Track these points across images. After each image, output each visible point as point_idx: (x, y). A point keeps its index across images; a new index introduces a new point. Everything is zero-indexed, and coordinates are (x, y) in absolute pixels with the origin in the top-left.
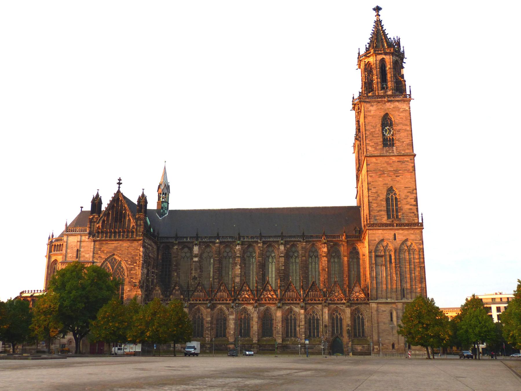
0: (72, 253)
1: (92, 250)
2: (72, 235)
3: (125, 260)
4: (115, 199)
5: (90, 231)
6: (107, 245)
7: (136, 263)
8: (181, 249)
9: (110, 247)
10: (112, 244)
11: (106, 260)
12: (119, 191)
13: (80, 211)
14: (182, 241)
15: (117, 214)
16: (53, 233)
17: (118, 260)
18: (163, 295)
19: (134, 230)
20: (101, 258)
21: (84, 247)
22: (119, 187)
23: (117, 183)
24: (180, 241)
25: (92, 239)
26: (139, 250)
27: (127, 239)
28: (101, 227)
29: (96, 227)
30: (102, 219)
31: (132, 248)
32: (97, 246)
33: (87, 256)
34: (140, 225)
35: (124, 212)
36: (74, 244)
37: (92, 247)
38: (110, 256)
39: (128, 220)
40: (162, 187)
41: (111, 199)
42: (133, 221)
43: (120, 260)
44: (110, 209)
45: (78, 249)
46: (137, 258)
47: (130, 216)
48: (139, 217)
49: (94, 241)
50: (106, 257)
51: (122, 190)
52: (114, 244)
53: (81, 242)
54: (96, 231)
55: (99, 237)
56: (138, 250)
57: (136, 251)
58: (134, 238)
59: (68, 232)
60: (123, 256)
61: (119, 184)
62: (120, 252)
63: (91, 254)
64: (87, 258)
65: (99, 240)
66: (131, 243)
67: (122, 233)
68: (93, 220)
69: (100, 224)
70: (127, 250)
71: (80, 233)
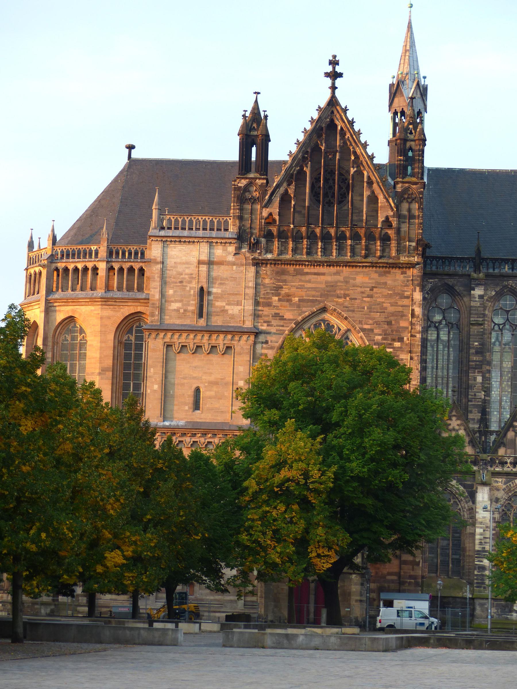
0: (181, 301)
1: (251, 292)
2: (179, 240)
3: (363, 330)
4: (321, 129)
5: (240, 228)
6: (299, 277)
7: (401, 340)
8: (491, 298)
9: (309, 285)
10: (315, 274)
11: (299, 325)
12: (333, 102)
13: (125, 160)
14: (497, 271)
15: (329, 173)
16: (53, 230)
17: (340, 330)
18: (473, 446)
19: (390, 232)
20: (282, 318)
21: (223, 282)
22: (334, 88)
23: (327, 75)
24: (491, 271)
25: (248, 255)
26: (411, 298)
27: (369, 259)
28: (277, 218)
29: (261, 218)
30: (282, 190)
31: (386, 292)
32: (267, 281)
33: (233, 310)
34: (412, 217)
35: (352, 171)
36: (187, 271)
37: (251, 284)
38: (313, 315)
39: (369, 197)
40: (409, 91)
41: (309, 127)
42: (388, 201)
43: (344, 327)
44: (304, 159)
45: (202, 289)
46: (404, 324)
47: (375, 186)
48: (405, 190)
49: (257, 263)
50: (300, 318)
51: (343, 101)
52: (323, 274)
53: (210, 263)
54: (260, 230)
55: (271, 252)
56: (408, 297)
57: (400, 303)
58: (390, 257)
59: (163, 228)
60: (357, 316)
61: (334, 75)
62: (346, 304)
63: (249, 306)
64: (232, 317)
65: (275, 262)
66: (380, 275)
67: (349, 242)
68: (248, 195)
69: (275, 209)
70: (368, 296)
71: (208, 233)
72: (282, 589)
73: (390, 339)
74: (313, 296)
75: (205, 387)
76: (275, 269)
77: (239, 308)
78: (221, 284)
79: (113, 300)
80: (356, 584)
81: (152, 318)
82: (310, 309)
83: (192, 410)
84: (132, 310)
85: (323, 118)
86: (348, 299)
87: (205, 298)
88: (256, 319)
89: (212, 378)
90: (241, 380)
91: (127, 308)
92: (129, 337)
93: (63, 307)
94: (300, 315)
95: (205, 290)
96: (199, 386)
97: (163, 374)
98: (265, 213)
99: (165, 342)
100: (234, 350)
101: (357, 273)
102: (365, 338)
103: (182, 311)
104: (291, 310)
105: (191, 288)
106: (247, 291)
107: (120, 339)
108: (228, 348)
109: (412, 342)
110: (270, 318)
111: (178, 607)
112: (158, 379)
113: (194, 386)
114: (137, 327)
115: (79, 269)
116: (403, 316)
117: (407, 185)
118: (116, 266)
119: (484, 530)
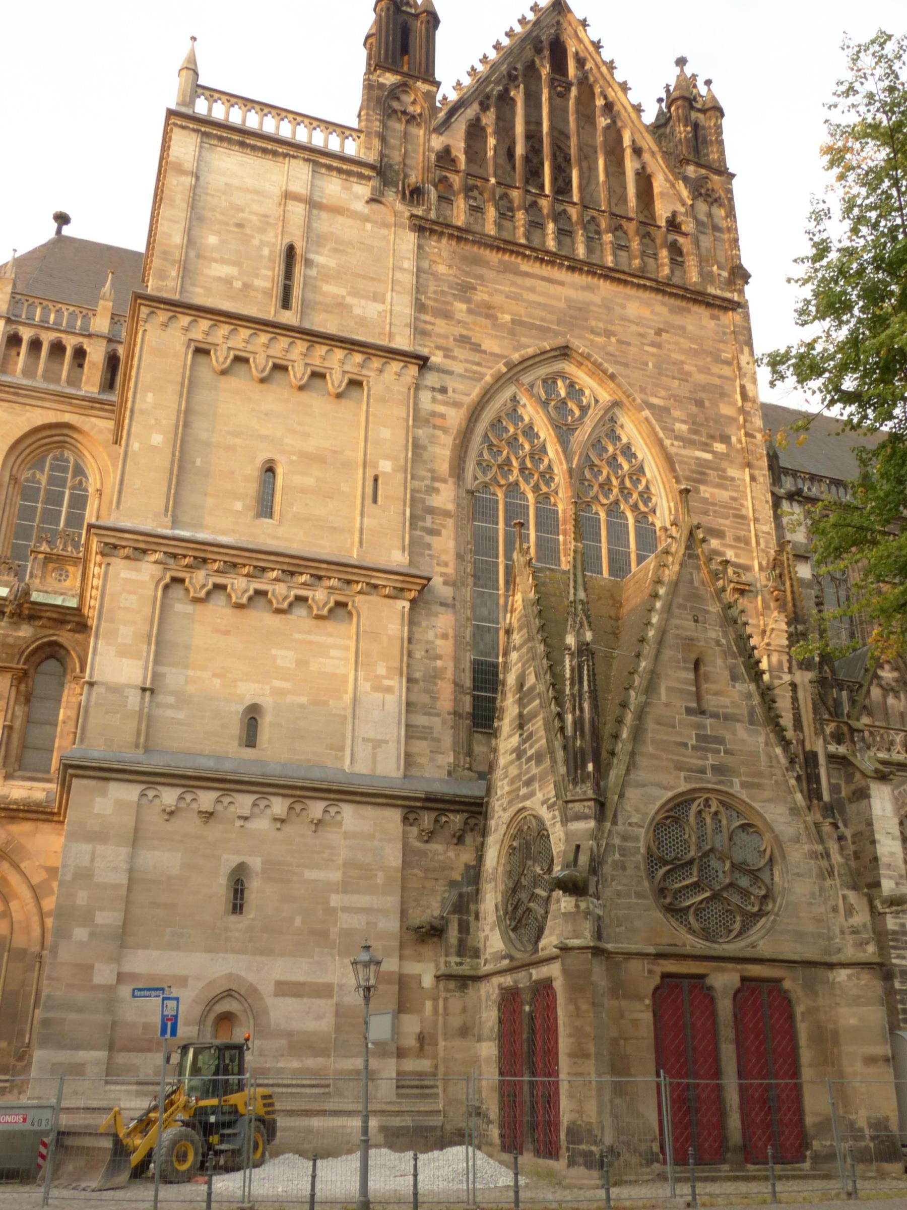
0: (236, 263)
1: (407, 280)
3: (651, 406)
6: (511, 277)
7: (725, 439)
9: (532, 297)
10: (544, 279)
20: (476, 348)
28: (462, 158)
31: (686, 344)
32: (442, 269)
36: (255, 207)
37: (409, 264)
38: (541, 358)
45: (290, 251)
46: (726, 410)
50: (516, 357)
52: (561, 283)
54: (427, 169)
56: (728, 363)
57: (715, 369)
62: (611, 349)
63: (404, 308)
64: (362, 322)
66: (672, 310)
70: (653, 344)
72: (635, 1023)
73: (704, 434)
74: (542, 319)
75: (292, 463)
76: (458, 250)
77: (380, 307)
78: (336, 250)
79: (12, 390)
80: (856, 1001)
81: (161, 283)
82: (537, 342)
83: (251, 514)
84: (52, 417)
85: (543, 24)
86: (613, 340)
87: (299, 270)
88: (418, 337)
89: (310, 445)
90: (386, 457)
91: (39, 411)
92: (34, 474)
94: (516, 349)
95: (298, 251)
96: (276, 457)
97: (179, 411)
98: (437, 142)
99: (190, 340)
100: (369, 390)
101: (628, 297)
102: (654, 422)
103: (238, 284)
104: (497, 337)
105: (263, 244)
106: (399, 275)
107: (14, 472)
108: (355, 384)
109: (751, 447)
110: (451, 343)
111: (214, 1102)
112: (164, 422)
113: (262, 457)
114: (55, 458)
116: (723, 395)
117: (703, 171)
118: (26, 334)
119: (897, 884)
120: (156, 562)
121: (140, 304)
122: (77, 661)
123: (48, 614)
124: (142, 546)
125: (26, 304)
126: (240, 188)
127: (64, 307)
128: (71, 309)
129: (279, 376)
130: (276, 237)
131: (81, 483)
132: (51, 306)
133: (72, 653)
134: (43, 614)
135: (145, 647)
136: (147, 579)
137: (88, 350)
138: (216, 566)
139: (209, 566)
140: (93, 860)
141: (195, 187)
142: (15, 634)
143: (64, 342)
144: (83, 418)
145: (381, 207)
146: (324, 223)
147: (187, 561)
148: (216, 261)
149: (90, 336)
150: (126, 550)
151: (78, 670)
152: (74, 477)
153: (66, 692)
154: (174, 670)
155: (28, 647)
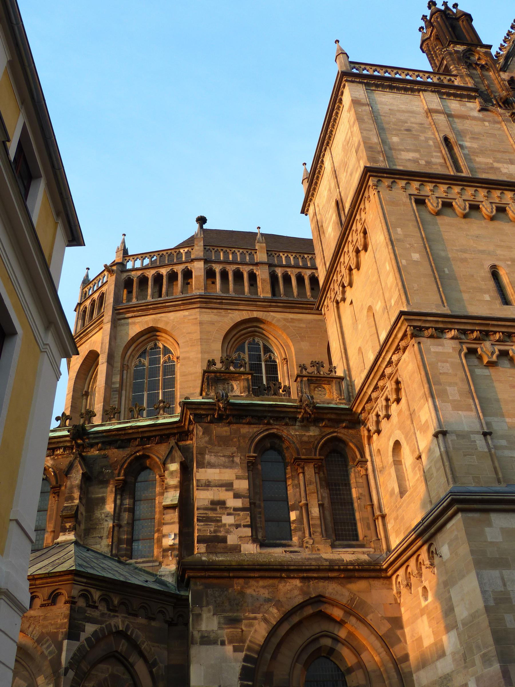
36: (413, 120)
75: (508, 266)
78: (474, 138)
79: (218, 301)
84: (245, 315)
91: (237, 312)
93: (139, 318)
95: (452, 140)
96: (496, 263)
105: (427, 139)
107: (228, 354)
114: (250, 344)
115: (162, 276)
118: (217, 268)
120: (453, 338)
121: (370, 176)
122: (356, 450)
123: (329, 416)
124: (441, 326)
125: (213, 252)
126: (399, 111)
127: (236, 251)
128: (241, 251)
129: (474, 213)
130: (434, 134)
131: (270, 357)
132: (228, 251)
133: (351, 444)
134: (325, 416)
135: (471, 401)
136: (451, 351)
137: (257, 273)
138: (497, 336)
139: (492, 338)
140: (505, 585)
141: (373, 112)
142: (307, 434)
143: (241, 270)
144: (265, 313)
145: (489, 113)
146: (459, 124)
147: (475, 334)
148: (403, 151)
149: (257, 264)
150: (430, 331)
151: (359, 456)
152: (265, 354)
153: (352, 475)
154: (496, 419)
155: (318, 443)
